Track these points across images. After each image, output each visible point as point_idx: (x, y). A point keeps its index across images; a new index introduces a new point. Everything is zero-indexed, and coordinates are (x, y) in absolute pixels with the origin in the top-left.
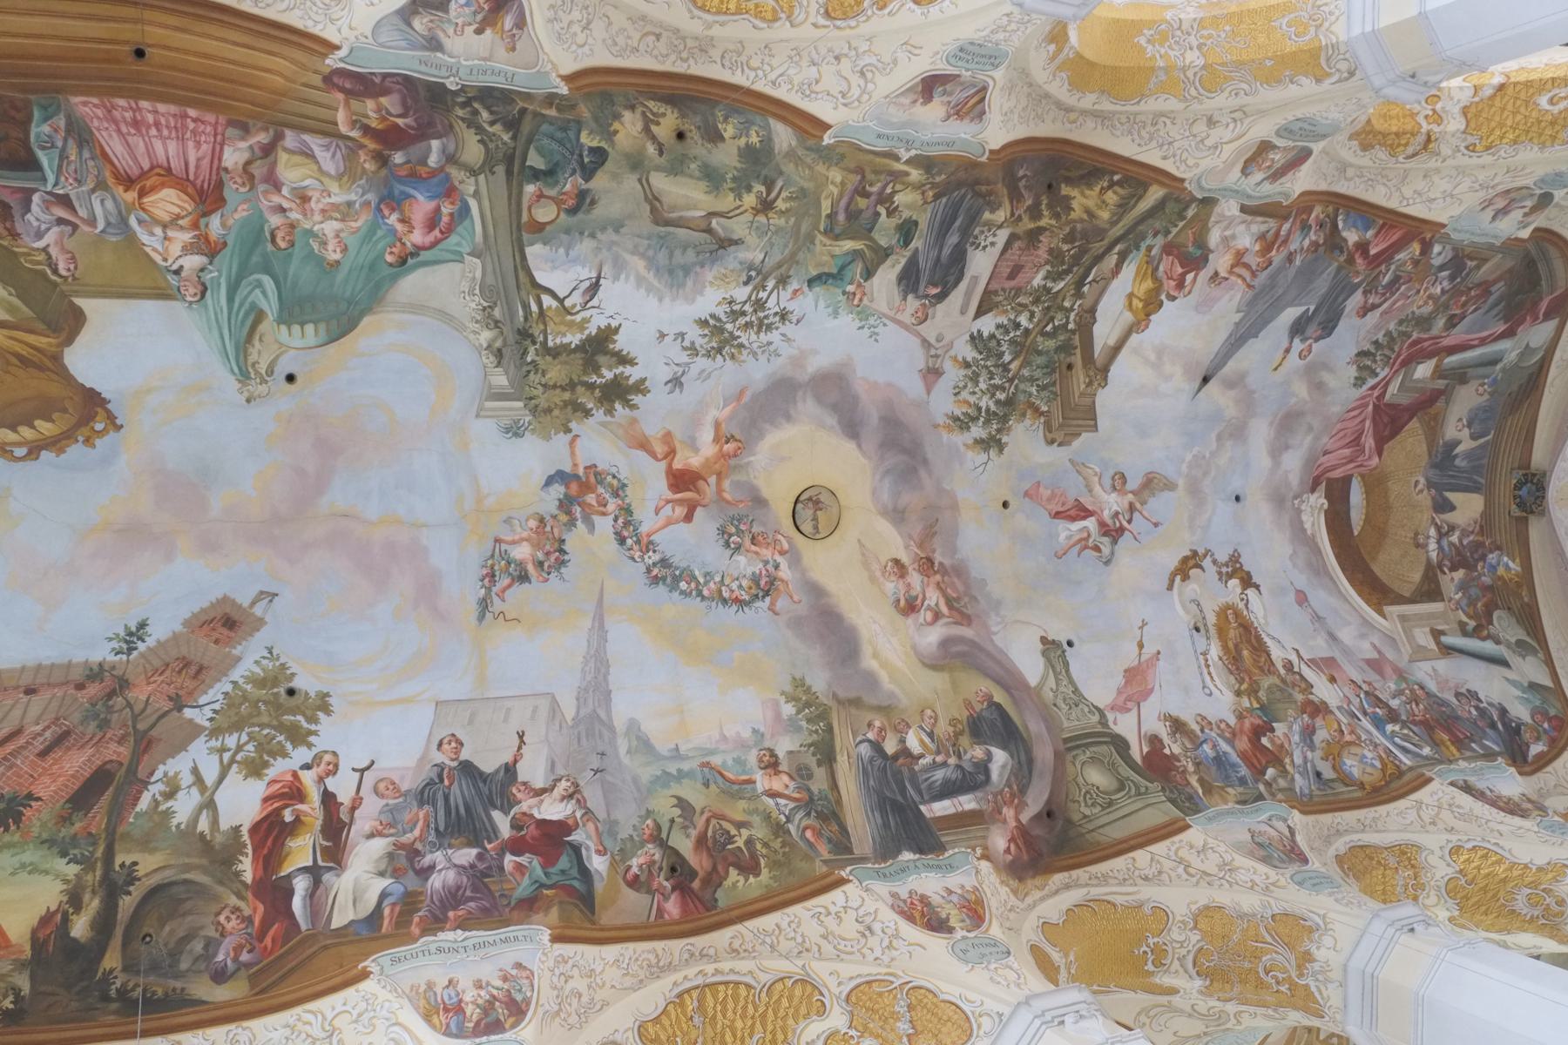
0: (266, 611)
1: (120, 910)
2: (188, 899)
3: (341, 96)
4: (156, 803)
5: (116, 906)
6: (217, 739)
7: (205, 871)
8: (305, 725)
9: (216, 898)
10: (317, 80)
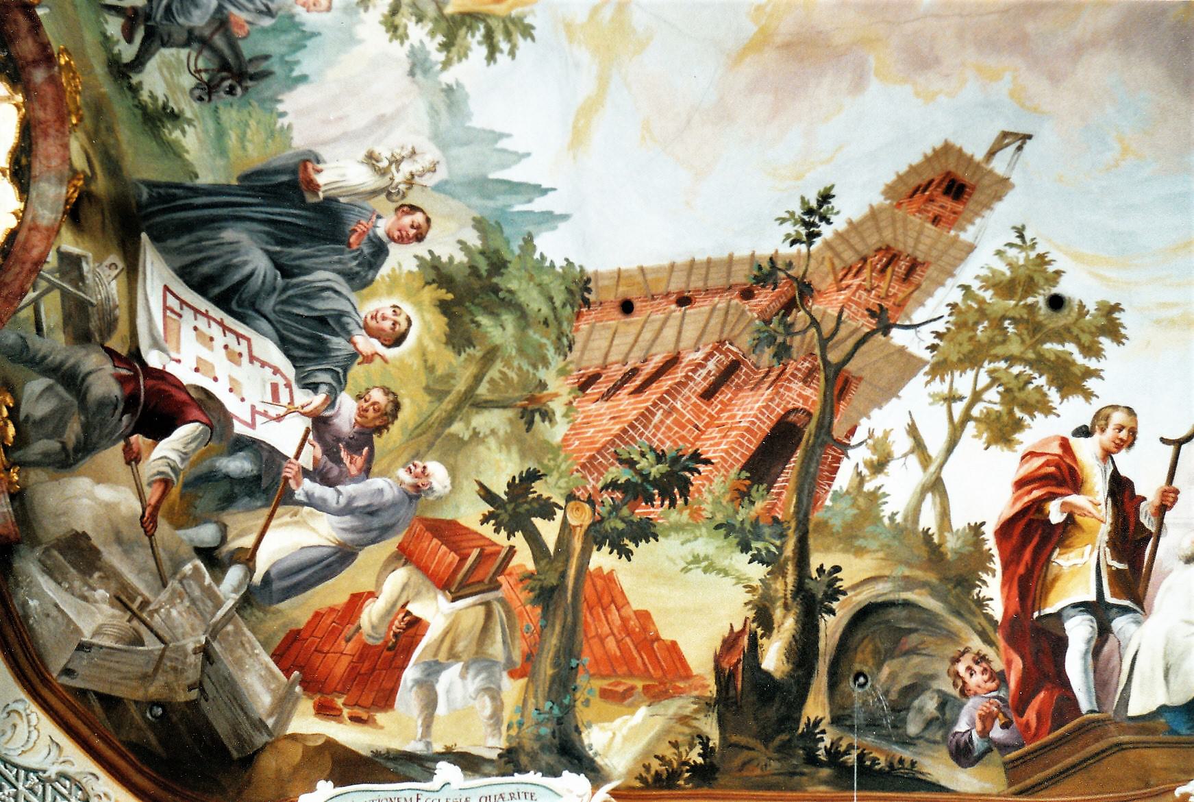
0: (1012, 165)
1: (822, 634)
2: (916, 630)
4: (862, 480)
5: (816, 629)
6: (943, 380)
7: (934, 592)
8: (1079, 358)
9: (952, 636)
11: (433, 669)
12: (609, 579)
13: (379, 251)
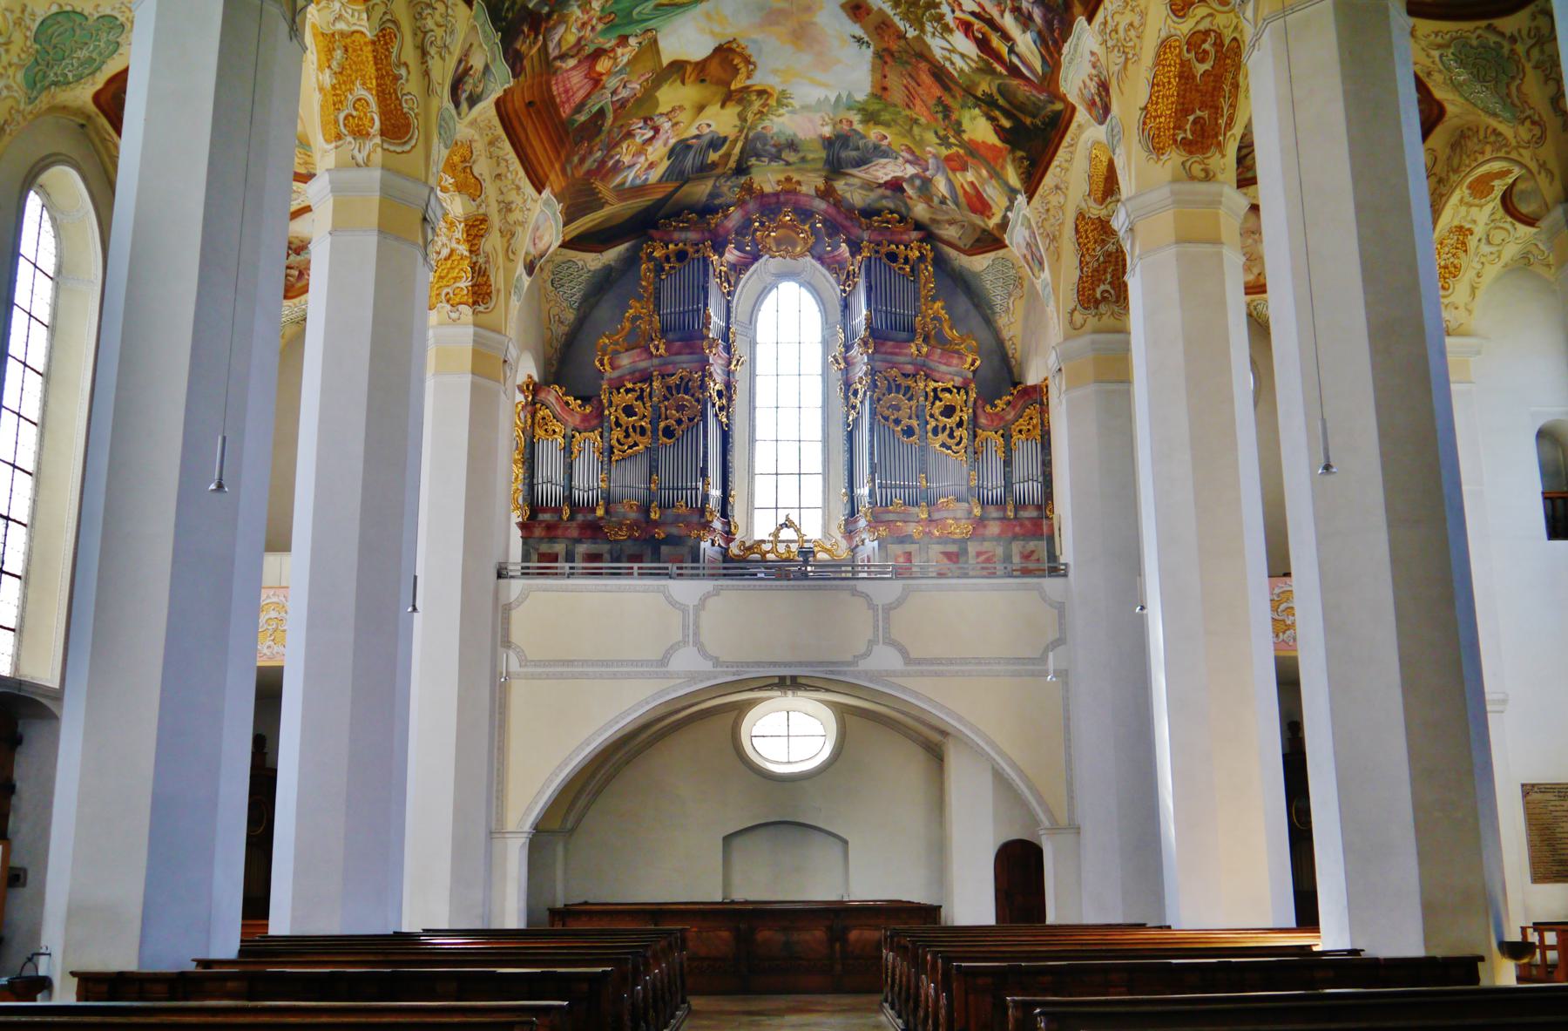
3: (525, 62)
10: (522, 78)
11: (985, 190)
12: (971, 141)
13: (855, 130)
